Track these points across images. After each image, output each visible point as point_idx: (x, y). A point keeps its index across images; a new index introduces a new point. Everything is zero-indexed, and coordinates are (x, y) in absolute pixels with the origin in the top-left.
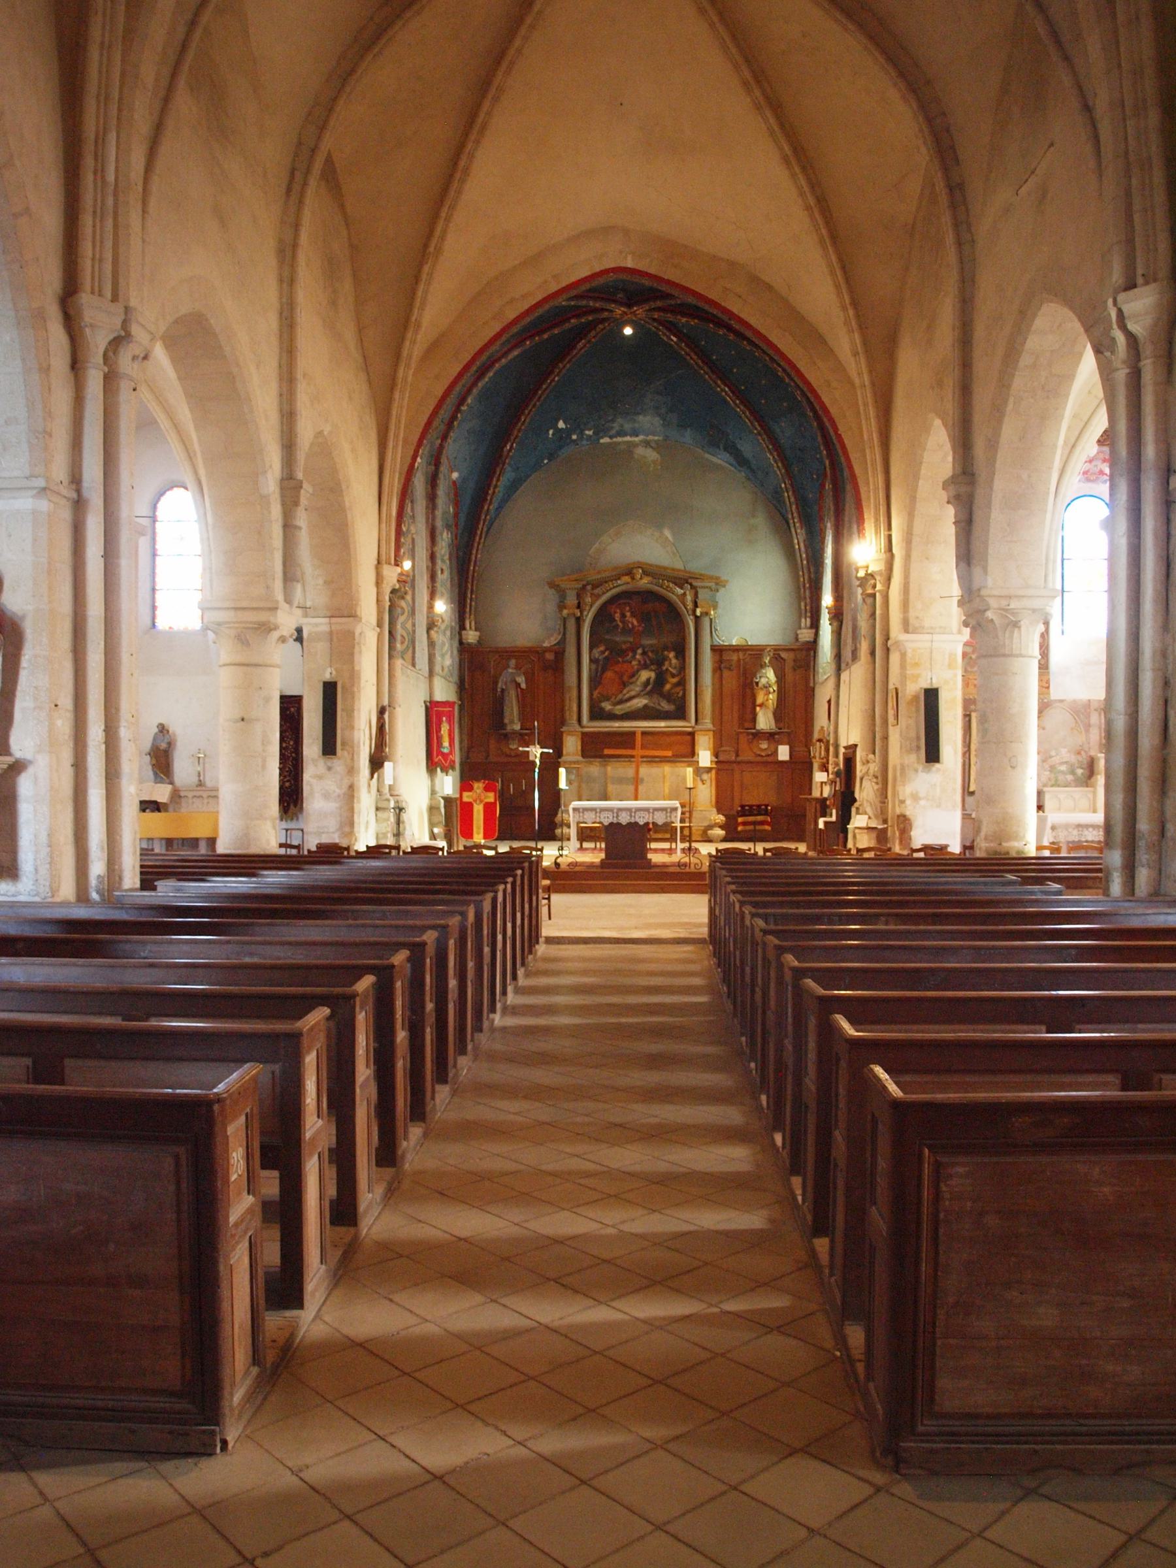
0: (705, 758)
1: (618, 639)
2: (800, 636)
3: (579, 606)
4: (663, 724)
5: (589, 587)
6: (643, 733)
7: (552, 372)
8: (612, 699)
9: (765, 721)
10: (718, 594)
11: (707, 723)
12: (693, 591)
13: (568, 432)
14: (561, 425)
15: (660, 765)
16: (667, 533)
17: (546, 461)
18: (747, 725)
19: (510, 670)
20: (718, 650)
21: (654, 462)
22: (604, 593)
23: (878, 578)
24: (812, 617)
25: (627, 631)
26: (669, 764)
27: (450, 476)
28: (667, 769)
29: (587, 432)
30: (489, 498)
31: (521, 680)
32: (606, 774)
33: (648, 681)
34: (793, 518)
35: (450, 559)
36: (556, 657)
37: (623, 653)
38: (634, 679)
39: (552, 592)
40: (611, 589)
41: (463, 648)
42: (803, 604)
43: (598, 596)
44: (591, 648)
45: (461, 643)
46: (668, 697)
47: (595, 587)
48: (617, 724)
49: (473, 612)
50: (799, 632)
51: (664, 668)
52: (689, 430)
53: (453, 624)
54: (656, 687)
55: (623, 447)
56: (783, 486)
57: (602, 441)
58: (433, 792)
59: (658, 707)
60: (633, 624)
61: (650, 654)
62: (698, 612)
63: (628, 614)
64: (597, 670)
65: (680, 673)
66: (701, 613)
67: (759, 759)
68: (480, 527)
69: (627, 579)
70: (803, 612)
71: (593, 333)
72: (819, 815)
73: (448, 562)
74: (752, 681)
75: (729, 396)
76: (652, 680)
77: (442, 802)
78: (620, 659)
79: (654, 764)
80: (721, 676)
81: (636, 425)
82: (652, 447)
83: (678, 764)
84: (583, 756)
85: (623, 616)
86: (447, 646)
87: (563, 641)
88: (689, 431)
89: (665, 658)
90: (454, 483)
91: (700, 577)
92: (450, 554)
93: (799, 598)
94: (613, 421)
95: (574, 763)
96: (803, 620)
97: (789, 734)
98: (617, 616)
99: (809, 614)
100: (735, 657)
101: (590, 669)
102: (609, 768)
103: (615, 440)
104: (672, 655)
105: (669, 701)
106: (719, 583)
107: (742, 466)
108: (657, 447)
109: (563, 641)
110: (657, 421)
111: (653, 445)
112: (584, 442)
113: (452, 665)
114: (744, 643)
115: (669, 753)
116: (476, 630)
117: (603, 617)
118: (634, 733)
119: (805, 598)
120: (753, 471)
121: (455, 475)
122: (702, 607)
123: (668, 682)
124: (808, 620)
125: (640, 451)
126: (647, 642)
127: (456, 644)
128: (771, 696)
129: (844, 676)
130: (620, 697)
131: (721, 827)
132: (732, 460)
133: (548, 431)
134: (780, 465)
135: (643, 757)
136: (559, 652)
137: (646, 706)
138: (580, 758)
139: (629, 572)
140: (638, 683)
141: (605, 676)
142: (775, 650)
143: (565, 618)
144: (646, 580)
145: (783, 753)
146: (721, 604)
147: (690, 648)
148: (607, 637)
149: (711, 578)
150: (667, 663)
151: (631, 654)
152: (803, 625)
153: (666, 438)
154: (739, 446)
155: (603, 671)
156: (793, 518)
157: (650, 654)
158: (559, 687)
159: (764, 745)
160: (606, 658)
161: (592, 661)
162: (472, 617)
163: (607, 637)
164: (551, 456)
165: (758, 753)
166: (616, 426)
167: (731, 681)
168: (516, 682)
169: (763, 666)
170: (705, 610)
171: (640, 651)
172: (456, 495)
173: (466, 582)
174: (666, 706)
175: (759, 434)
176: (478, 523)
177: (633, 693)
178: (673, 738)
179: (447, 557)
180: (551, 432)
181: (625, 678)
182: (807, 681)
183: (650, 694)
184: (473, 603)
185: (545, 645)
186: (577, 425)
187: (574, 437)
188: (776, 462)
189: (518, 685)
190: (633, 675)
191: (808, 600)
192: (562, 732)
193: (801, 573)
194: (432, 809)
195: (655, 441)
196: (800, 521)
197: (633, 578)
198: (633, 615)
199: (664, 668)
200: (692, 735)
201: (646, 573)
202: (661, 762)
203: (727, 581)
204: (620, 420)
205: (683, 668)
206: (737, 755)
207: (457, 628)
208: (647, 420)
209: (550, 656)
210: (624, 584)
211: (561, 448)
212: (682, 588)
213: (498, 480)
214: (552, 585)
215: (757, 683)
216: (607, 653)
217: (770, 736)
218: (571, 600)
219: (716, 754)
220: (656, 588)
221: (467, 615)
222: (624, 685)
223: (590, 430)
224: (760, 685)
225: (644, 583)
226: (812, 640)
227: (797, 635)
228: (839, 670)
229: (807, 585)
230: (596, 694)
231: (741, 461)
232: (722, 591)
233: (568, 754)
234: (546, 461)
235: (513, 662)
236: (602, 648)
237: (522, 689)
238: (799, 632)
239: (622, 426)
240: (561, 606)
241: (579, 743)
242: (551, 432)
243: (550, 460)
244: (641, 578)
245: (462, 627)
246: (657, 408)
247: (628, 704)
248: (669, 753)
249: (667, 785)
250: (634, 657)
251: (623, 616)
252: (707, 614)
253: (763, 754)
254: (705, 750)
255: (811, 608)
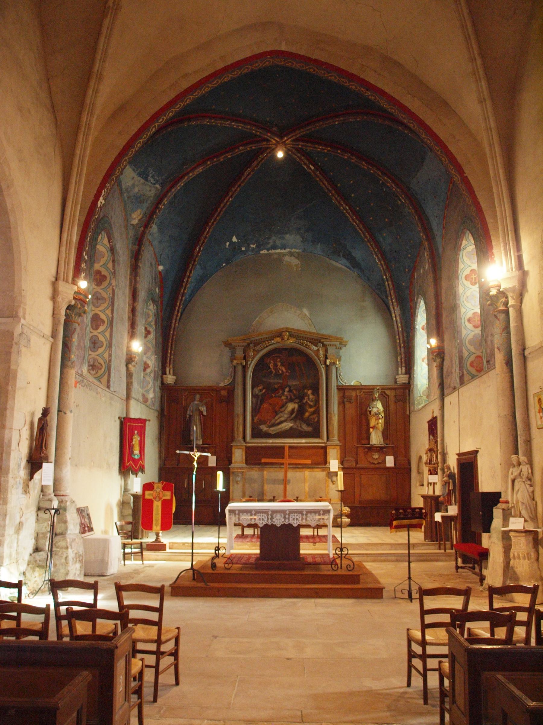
0: (334, 465)
1: (272, 381)
2: (398, 380)
3: (245, 358)
4: (303, 441)
5: (252, 345)
6: (290, 447)
7: (227, 194)
8: (268, 423)
9: (376, 438)
10: (341, 351)
11: (335, 439)
12: (324, 349)
13: (240, 245)
14: (234, 239)
15: (301, 470)
16: (306, 311)
17: (224, 265)
18: (363, 442)
19: (196, 402)
20: (342, 389)
21: (296, 265)
22: (262, 349)
23: (510, 295)
24: (406, 367)
25: (277, 375)
26: (309, 470)
27: (157, 268)
28: (307, 473)
29: (252, 246)
30: (184, 284)
31: (203, 409)
32: (263, 476)
33: (293, 411)
34: (392, 300)
35: (156, 324)
36: (228, 393)
37: (276, 390)
38: (283, 409)
39: (227, 349)
40: (268, 346)
41: (164, 387)
42: (399, 358)
43: (258, 352)
44: (253, 388)
45: (162, 383)
46: (308, 422)
47: (256, 344)
48: (271, 441)
49: (172, 362)
50: (397, 377)
51: (304, 401)
52: (319, 244)
53: (156, 369)
54: (299, 415)
55: (276, 256)
56: (385, 277)
57: (262, 252)
58: (126, 490)
59: (300, 428)
60: (282, 371)
61: (295, 392)
62: (328, 362)
63: (279, 364)
64: (257, 403)
65: (315, 405)
66: (330, 363)
67: (373, 466)
68: (178, 304)
69: (278, 339)
70: (400, 363)
71: (255, 163)
72: (434, 509)
73: (154, 326)
74: (366, 410)
75: (348, 213)
76: (295, 410)
77: (132, 498)
78: (274, 395)
79: (298, 470)
80: (344, 407)
81: (284, 241)
82: (295, 256)
83: (315, 470)
84: (247, 463)
85: (276, 365)
86: (150, 385)
87: (233, 384)
88: (319, 246)
89: (306, 394)
90: (160, 273)
91: (329, 338)
92: (156, 321)
93: (396, 354)
94: (269, 238)
95: (241, 468)
96: (400, 369)
97: (393, 447)
98: (271, 366)
99: (403, 365)
100: (353, 394)
101: (252, 402)
102: (265, 473)
103: (270, 252)
104: (310, 392)
105: (308, 425)
106: (342, 343)
107: (354, 268)
108: (298, 256)
109: (233, 384)
110: (299, 238)
111: (296, 255)
112: (250, 253)
113: (155, 398)
114: (359, 384)
115: (309, 462)
116: (174, 375)
117: (262, 365)
118: (283, 448)
119: (401, 353)
120: (362, 271)
121: (161, 268)
122: (331, 359)
123: (307, 411)
124: (404, 369)
125: (287, 259)
126: (292, 383)
127: (158, 383)
128: (380, 421)
129: (447, 400)
130: (273, 421)
131: (348, 516)
132: (348, 264)
133: (225, 243)
134: (382, 262)
135: (289, 464)
136: (231, 390)
137: (291, 428)
138: (244, 465)
139: (280, 334)
140: (286, 412)
141: (262, 406)
142: (382, 389)
143: (235, 366)
144: (291, 340)
145: (390, 461)
146: (343, 359)
147: (322, 388)
148: (264, 379)
149: (337, 339)
150: (306, 398)
151: (281, 392)
152: (400, 372)
153: (304, 251)
154: (353, 254)
155: (261, 404)
156: (392, 300)
157: (295, 392)
158: (230, 414)
159: (376, 456)
160: (263, 395)
161: (253, 396)
162: (171, 366)
163: (264, 379)
164: (228, 261)
165: (372, 462)
166: (271, 242)
167: (351, 410)
168: (199, 410)
169: (373, 400)
170: (333, 361)
171: (287, 390)
172: (161, 281)
173: (168, 342)
174: (305, 428)
175: (369, 241)
176: (176, 302)
177: (282, 419)
178: (311, 451)
179: (153, 323)
180: (228, 244)
181: (277, 408)
182: (405, 413)
183: (295, 419)
184: (172, 357)
185: (220, 385)
186: (245, 240)
187: (243, 249)
188: (380, 261)
189: (201, 412)
190: (283, 406)
191: (403, 356)
192: (232, 446)
193: (397, 337)
194: (123, 504)
195: (297, 253)
196: (397, 301)
197: (282, 339)
198: (282, 365)
199: (304, 401)
200: (325, 448)
201: (291, 335)
202: (303, 468)
203: (347, 342)
204: (274, 238)
205: (317, 401)
206: (357, 463)
207: (160, 373)
208: (291, 238)
209: (224, 393)
210: (277, 343)
211: (234, 256)
212: (316, 346)
213: (190, 273)
214: (227, 344)
215: (370, 412)
216: (264, 391)
217: (380, 449)
218: (239, 353)
219: (342, 462)
220: (298, 346)
221: (168, 365)
222: (276, 413)
223: (254, 244)
224: (372, 413)
225: (290, 342)
226: (407, 382)
227: (396, 379)
228: (442, 396)
229: (402, 345)
230: (256, 419)
231: (355, 264)
232: (344, 349)
233: (236, 462)
234: (224, 265)
235: (198, 397)
236: (261, 387)
237: (203, 416)
238: (397, 377)
239: (275, 242)
240: (232, 358)
241: (244, 455)
242: (228, 244)
243: (227, 264)
244: (288, 339)
245: (164, 373)
246: (298, 229)
247: (279, 427)
248: (309, 462)
249: (307, 485)
250: (283, 394)
251: (276, 365)
252: (334, 363)
253: (376, 463)
254: (334, 459)
255: (405, 360)
